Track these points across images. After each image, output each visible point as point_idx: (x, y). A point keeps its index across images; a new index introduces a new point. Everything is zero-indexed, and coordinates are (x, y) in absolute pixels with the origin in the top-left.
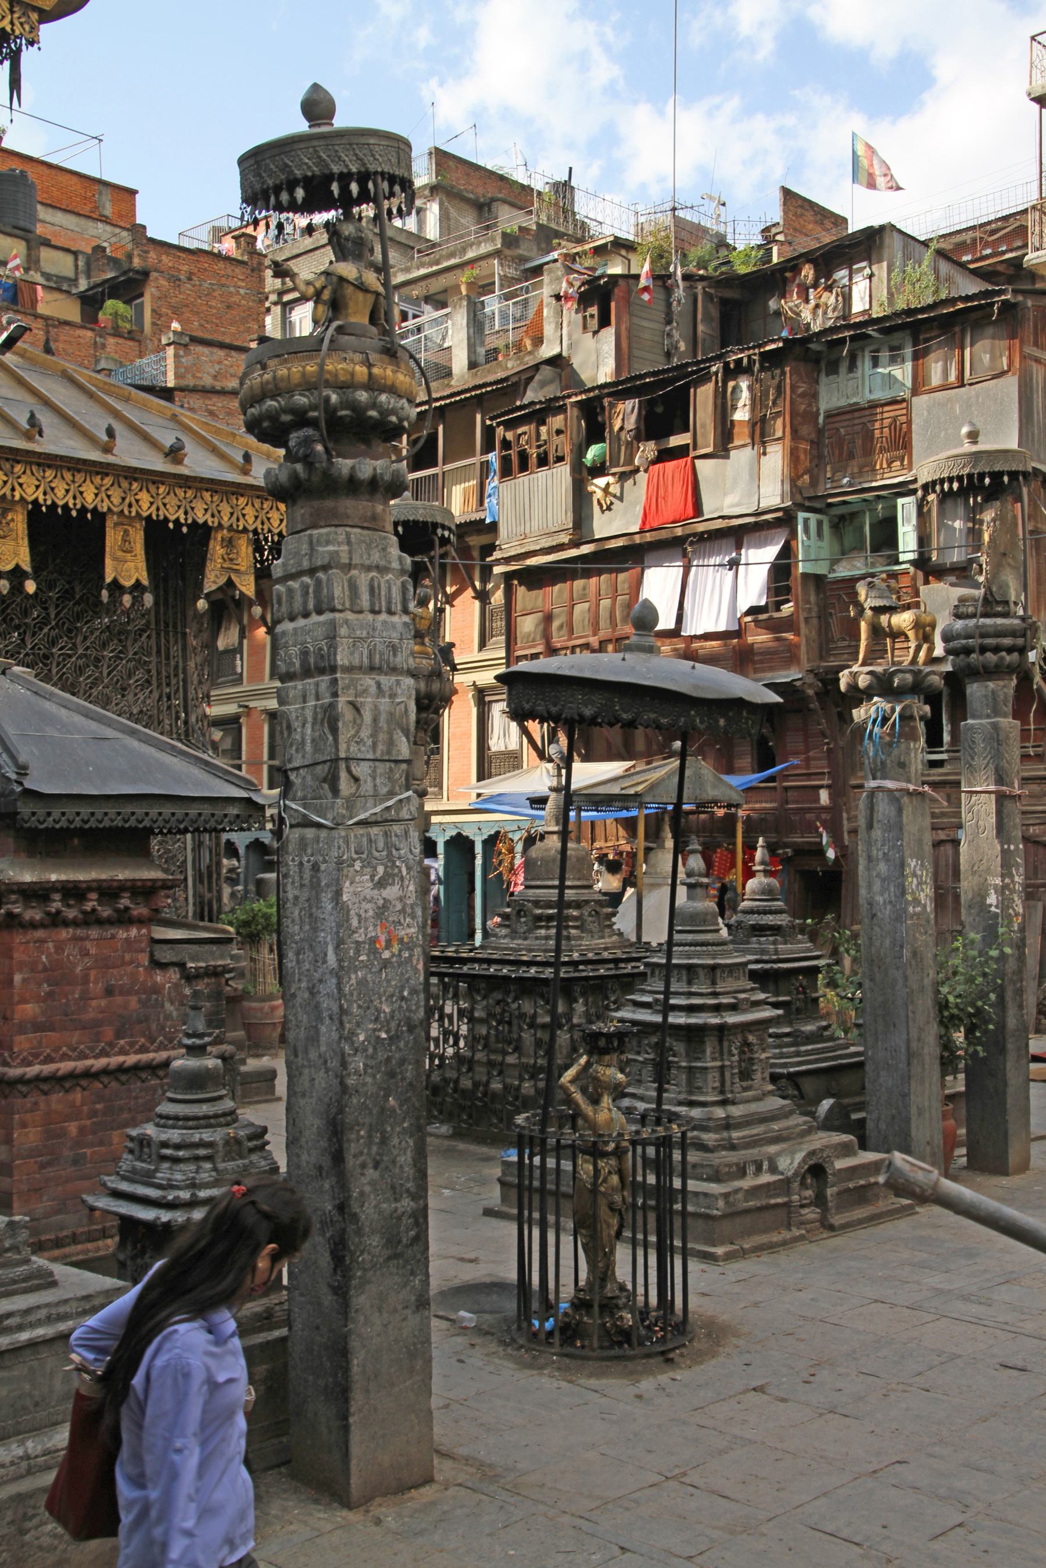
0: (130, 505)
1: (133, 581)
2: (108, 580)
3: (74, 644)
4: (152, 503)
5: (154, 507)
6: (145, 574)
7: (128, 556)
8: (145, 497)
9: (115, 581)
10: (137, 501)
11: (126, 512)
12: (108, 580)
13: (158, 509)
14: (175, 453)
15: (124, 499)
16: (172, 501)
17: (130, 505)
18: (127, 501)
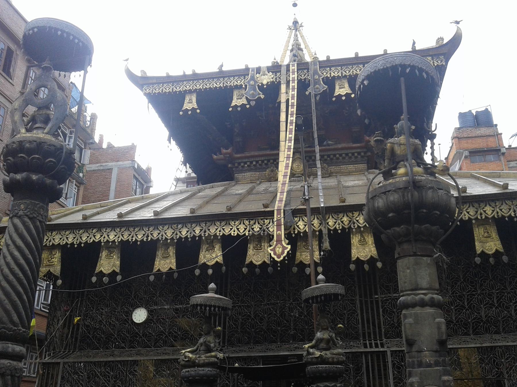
0: (481, 214)
1: (494, 251)
2: (479, 252)
3: (476, 289)
4: (493, 211)
5: (495, 212)
6: (501, 246)
7: (489, 239)
8: (489, 210)
9: (483, 252)
10: (485, 211)
11: (479, 218)
12: (479, 252)
13: (497, 213)
14: (506, 186)
15: (477, 212)
16: (505, 207)
17: (481, 214)
18: (479, 212)
